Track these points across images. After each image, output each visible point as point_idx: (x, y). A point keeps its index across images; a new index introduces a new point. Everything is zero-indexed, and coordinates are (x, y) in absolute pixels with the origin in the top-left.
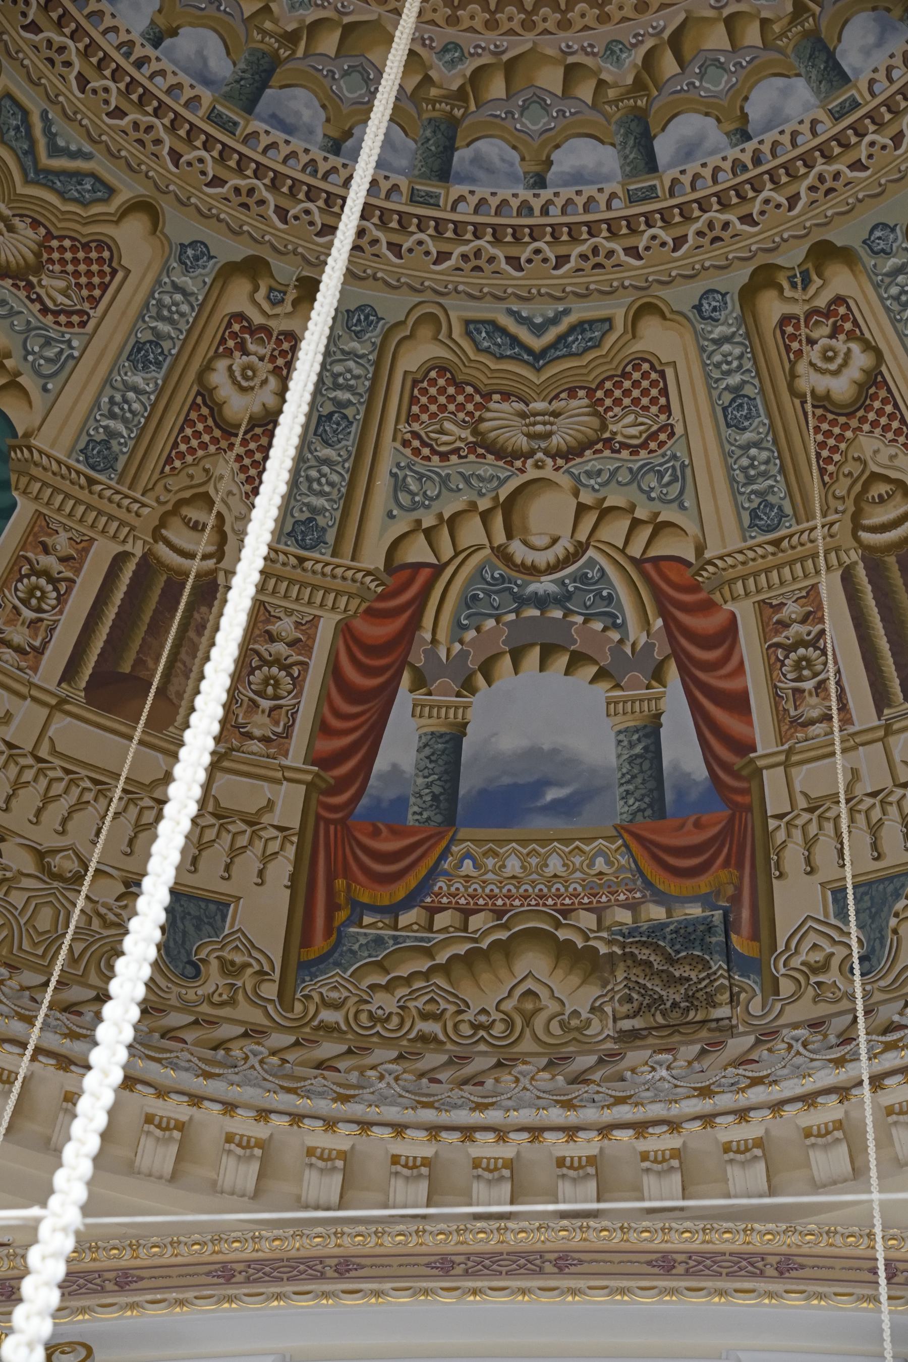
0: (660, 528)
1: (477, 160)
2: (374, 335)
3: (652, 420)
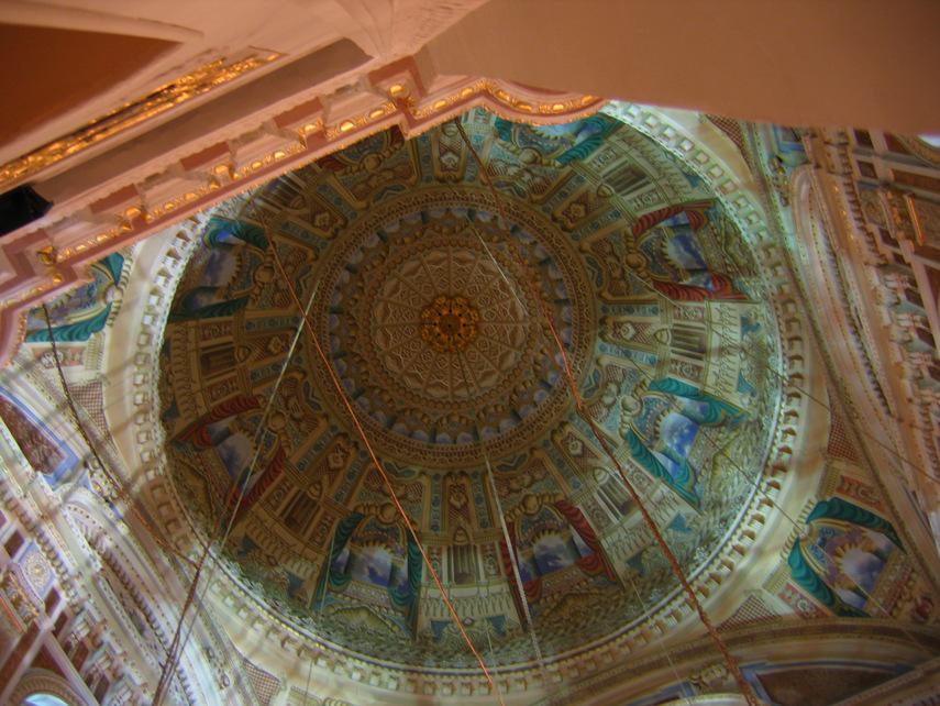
0: (346, 173)
2: (424, 178)
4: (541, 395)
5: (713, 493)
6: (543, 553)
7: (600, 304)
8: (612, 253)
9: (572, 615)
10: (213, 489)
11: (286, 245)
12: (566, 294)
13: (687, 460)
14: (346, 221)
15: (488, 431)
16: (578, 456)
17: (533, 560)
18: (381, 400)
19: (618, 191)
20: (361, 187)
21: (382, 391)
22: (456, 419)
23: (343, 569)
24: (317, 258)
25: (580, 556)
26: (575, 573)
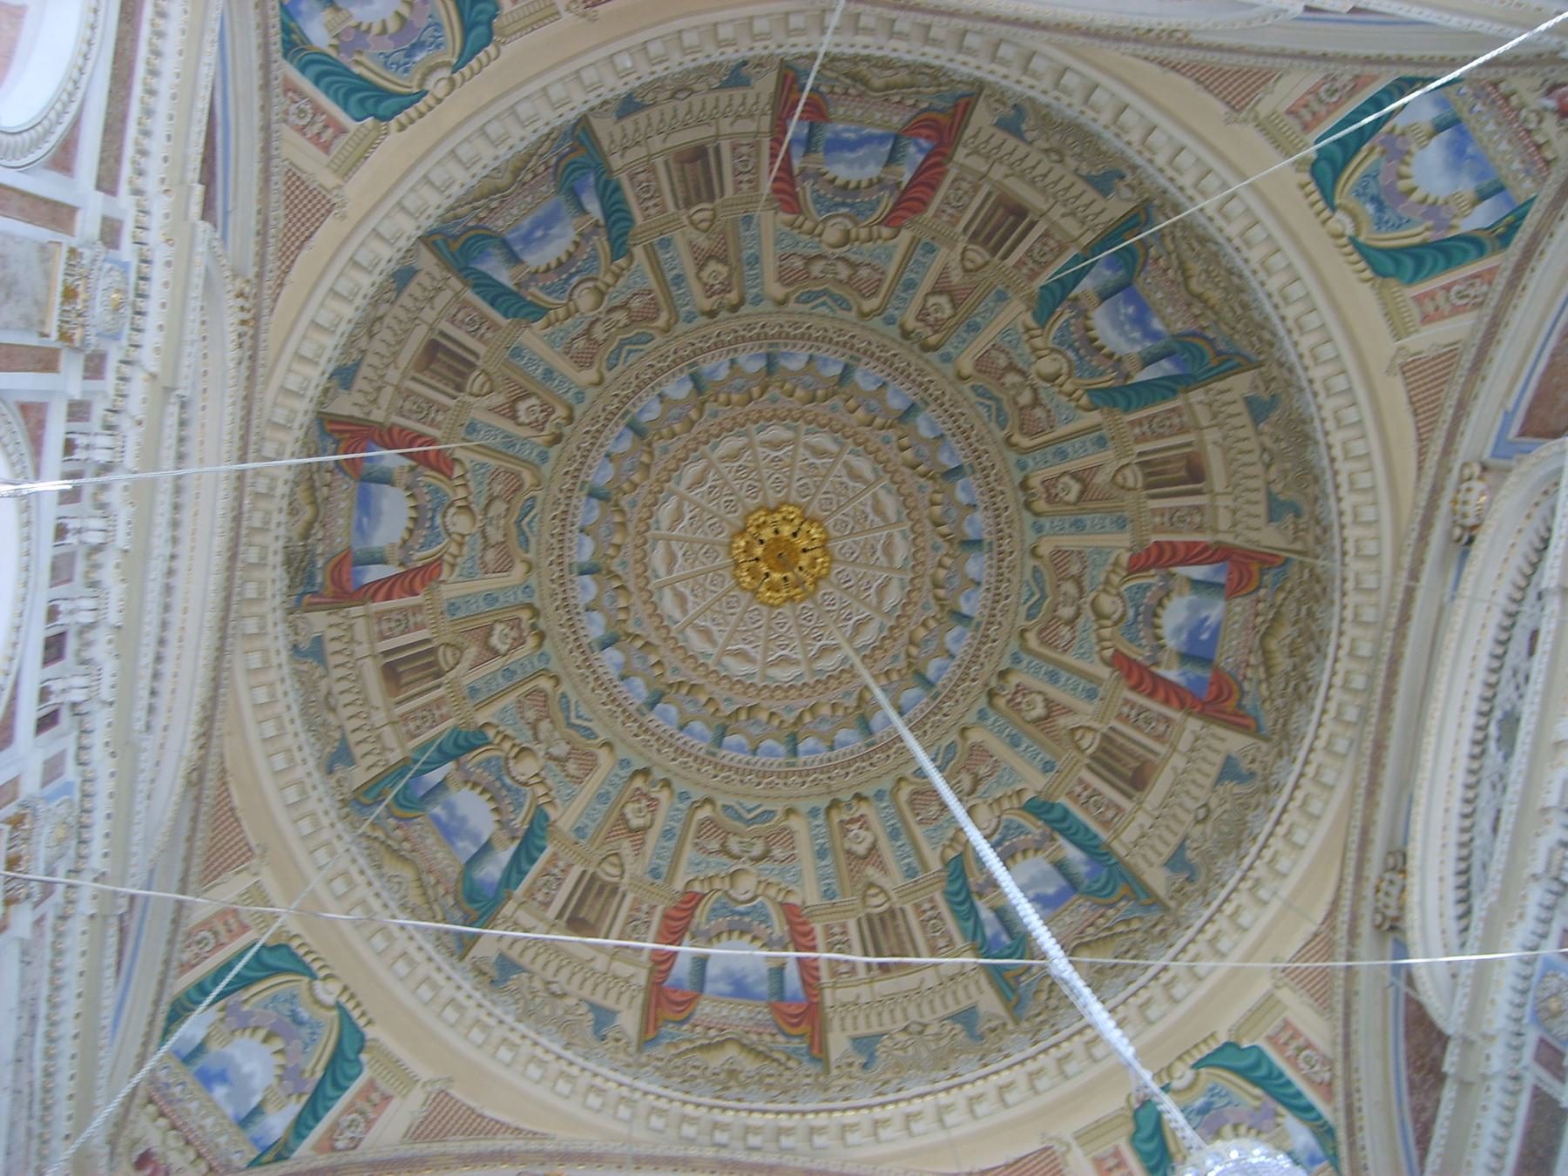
0: (453, 566)
1: (591, 510)
2: (537, 461)
3: (491, 566)
4: (964, 489)
5: (1239, 326)
6: (1184, 636)
7: (877, 322)
8: (809, 260)
9: (1291, 655)
10: (754, 1037)
11: (504, 710)
12: (836, 362)
13: (1174, 336)
14: (530, 606)
15: (968, 599)
16: (1082, 492)
17: (1186, 657)
18: (823, 719)
19: (711, 198)
20: (490, 555)
21: (812, 709)
22: (922, 633)
23: (1005, 938)
24: (557, 680)
25: (1221, 586)
26: (1238, 609)
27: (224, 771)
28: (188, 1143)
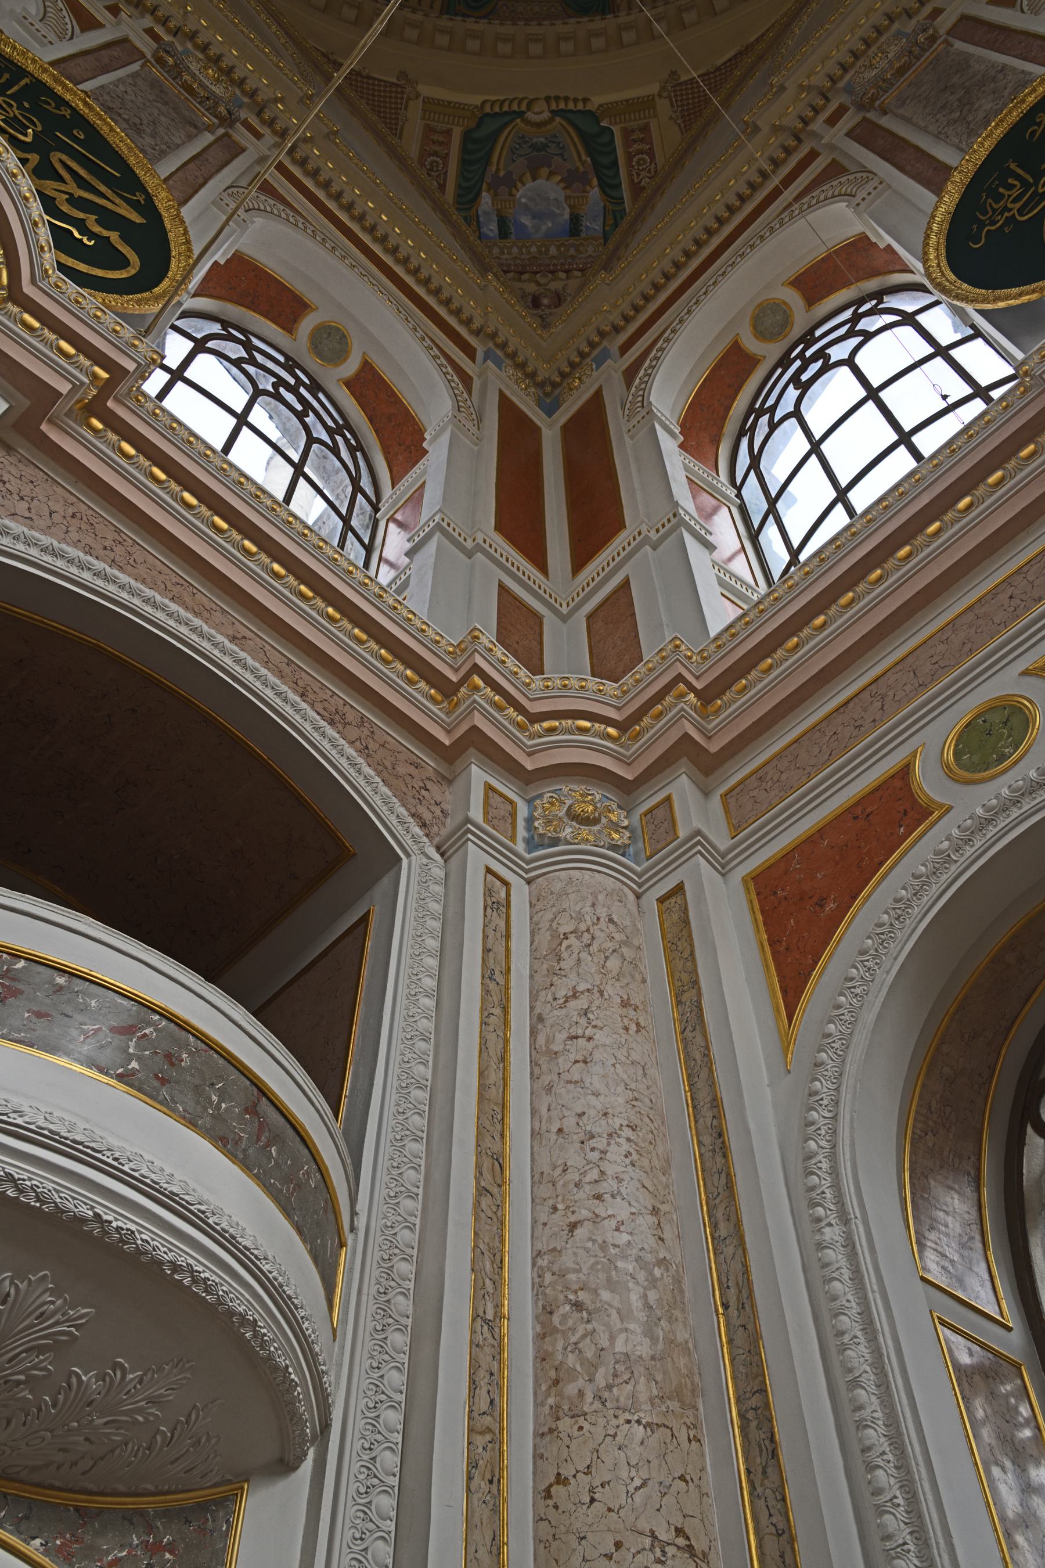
27: (324, 55)
28: (552, 272)
